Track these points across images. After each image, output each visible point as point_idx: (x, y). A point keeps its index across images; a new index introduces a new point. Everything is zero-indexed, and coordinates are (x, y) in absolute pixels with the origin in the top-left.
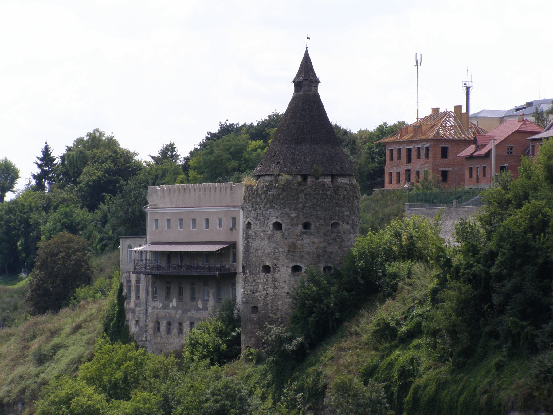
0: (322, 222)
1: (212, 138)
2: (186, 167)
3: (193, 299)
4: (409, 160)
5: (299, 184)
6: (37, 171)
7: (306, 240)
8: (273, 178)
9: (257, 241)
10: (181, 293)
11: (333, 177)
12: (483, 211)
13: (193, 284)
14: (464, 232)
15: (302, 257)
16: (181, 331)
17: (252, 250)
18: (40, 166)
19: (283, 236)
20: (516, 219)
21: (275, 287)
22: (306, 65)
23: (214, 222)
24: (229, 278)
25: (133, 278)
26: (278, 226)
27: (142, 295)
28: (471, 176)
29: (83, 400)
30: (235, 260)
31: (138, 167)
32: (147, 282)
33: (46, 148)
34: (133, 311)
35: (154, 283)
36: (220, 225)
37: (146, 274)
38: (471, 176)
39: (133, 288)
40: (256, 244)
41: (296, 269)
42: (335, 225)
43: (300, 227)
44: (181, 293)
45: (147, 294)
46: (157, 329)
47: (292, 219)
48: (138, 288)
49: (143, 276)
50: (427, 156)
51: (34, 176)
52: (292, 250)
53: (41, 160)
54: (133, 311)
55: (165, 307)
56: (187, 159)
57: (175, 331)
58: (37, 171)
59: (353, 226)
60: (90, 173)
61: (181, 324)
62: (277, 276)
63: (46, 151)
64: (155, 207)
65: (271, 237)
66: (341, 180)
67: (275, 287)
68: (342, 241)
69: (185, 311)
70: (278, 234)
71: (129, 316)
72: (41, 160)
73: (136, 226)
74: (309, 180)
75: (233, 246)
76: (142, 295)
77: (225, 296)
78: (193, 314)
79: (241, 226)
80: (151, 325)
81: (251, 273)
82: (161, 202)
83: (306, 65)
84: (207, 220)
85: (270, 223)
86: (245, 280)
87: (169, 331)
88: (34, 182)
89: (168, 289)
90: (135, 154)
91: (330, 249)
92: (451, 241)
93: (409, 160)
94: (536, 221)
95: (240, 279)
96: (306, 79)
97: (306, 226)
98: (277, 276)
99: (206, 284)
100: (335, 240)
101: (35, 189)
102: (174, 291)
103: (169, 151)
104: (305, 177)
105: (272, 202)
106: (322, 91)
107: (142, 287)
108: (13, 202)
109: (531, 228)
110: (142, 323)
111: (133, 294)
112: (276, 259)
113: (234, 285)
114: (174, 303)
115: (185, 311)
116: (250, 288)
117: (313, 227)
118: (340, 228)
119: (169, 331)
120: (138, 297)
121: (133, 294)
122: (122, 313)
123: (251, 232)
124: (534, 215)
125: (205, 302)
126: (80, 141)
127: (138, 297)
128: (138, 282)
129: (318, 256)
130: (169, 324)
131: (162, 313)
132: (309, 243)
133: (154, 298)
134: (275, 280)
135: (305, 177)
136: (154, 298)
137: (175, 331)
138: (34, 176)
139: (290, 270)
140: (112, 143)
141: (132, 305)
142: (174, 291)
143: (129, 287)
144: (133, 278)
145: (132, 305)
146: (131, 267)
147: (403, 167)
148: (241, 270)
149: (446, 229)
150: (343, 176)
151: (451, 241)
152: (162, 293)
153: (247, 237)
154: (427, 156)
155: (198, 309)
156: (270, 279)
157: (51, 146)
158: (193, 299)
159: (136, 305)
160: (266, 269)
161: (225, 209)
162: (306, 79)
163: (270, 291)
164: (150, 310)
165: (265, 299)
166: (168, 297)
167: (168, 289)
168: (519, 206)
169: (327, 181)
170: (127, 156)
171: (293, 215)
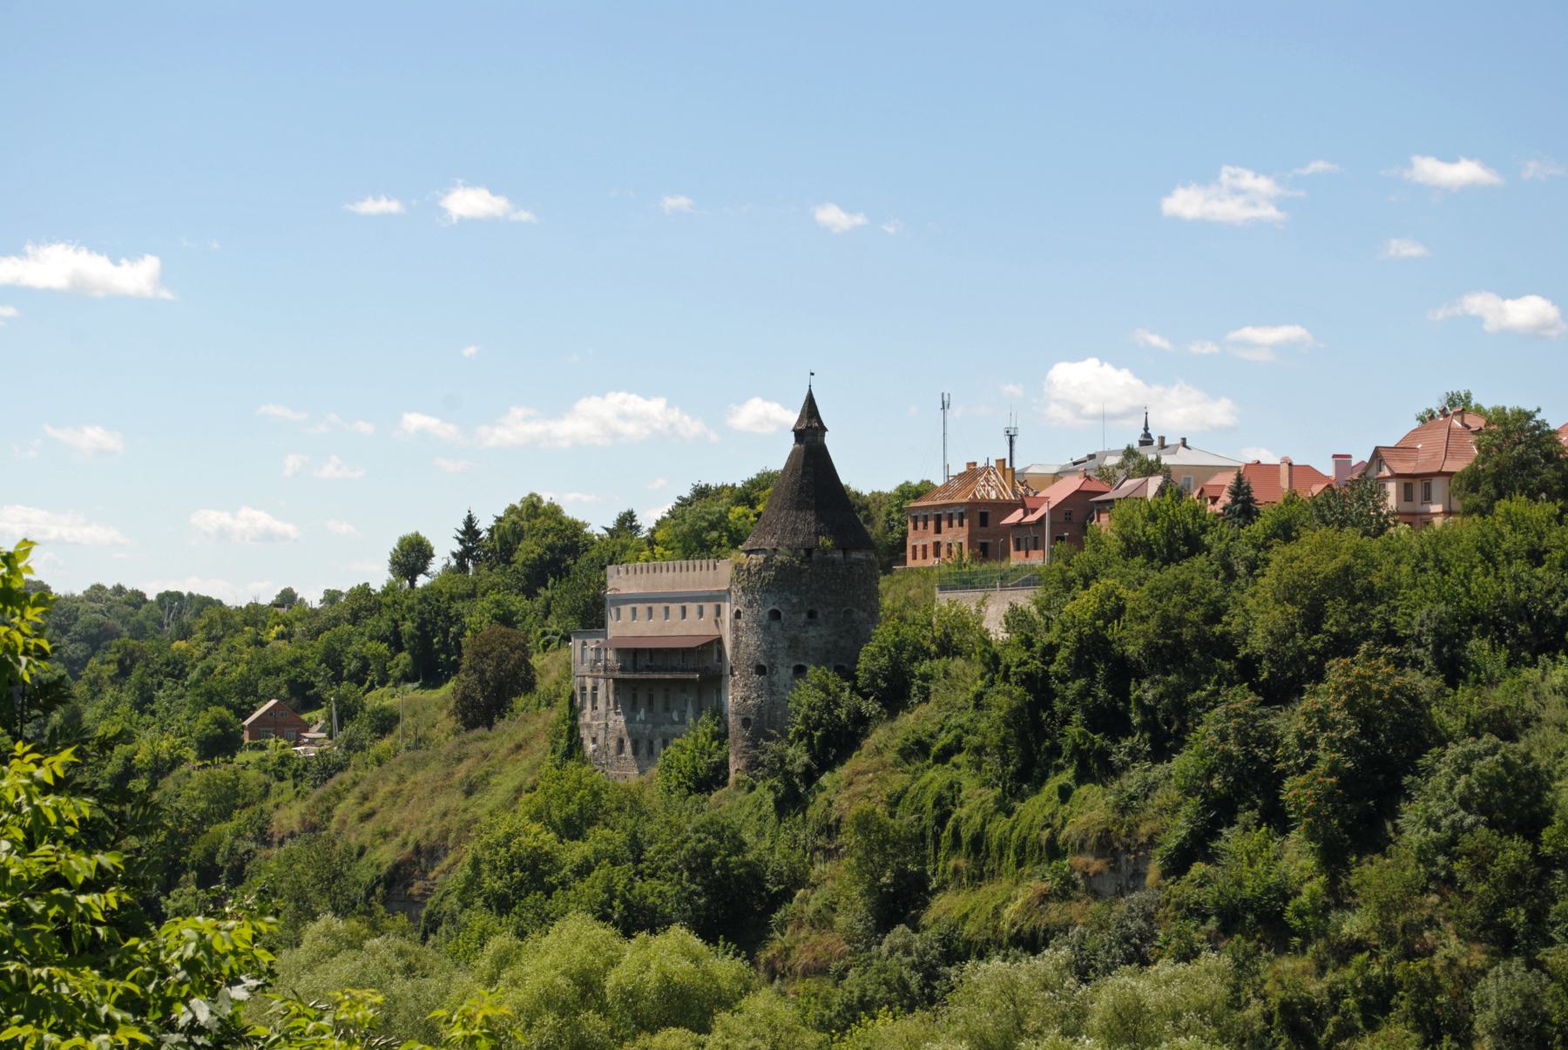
1: (684, 503)
2: (651, 542)
3: (667, 709)
7: (812, 632)
10: (651, 703)
12: (1039, 592)
15: (806, 654)
25: (589, 683)
29: (528, 841)
31: (590, 542)
39: (589, 697)
43: (804, 615)
44: (651, 703)
45: (608, 703)
46: (621, 748)
47: (794, 605)
48: (594, 696)
49: (601, 681)
52: (794, 644)
53: (463, 533)
54: (589, 726)
56: (653, 531)
58: (458, 548)
60: (528, 550)
61: (651, 743)
62: (775, 679)
66: (856, 555)
69: (656, 725)
71: (584, 733)
72: (463, 533)
76: (601, 706)
78: (667, 728)
80: (613, 744)
89: (635, 696)
92: (997, 631)
97: (812, 615)
98: (775, 679)
102: (642, 698)
103: (627, 522)
107: (601, 694)
110: (600, 741)
111: (589, 705)
113: (719, 691)
114: (642, 715)
115: (656, 725)
120: (594, 708)
121: (589, 705)
122: (573, 731)
125: (682, 713)
127: (594, 708)
128: (595, 688)
134: (772, 684)
139: (791, 671)
141: (587, 718)
142: (642, 698)
143: (583, 695)
150: (858, 549)
155: (673, 723)
157: (476, 515)
159: (593, 718)
167: (635, 696)
168: (1086, 587)
170: (577, 527)
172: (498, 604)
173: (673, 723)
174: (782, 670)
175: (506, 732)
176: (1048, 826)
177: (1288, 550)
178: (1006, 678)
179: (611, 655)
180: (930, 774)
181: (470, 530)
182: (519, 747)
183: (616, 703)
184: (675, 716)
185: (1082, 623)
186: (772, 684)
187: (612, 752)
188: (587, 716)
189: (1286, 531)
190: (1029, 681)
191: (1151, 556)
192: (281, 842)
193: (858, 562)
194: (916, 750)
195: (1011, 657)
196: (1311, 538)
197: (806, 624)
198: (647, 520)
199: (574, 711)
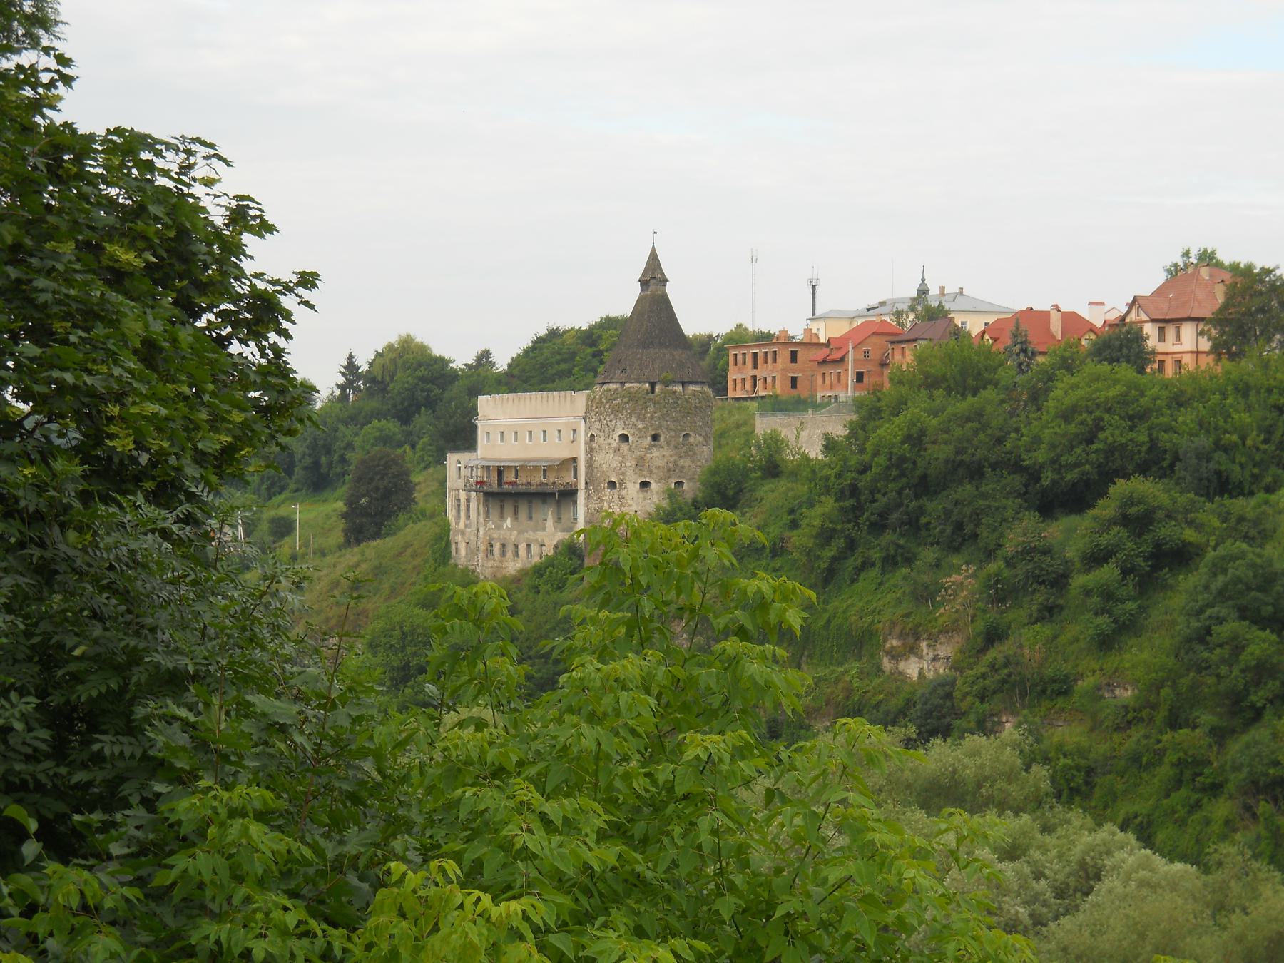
0: (673, 433)
7: (656, 453)
8: (618, 386)
9: (602, 455)
10: (516, 512)
11: (683, 383)
13: (530, 502)
14: (830, 445)
15: (651, 472)
16: (517, 554)
20: (890, 431)
21: (622, 505)
22: (653, 257)
23: (553, 434)
24: (568, 495)
25: (463, 496)
26: (624, 438)
30: (575, 477)
33: (351, 357)
34: (463, 533)
36: (560, 438)
39: (463, 507)
40: (599, 458)
41: (645, 485)
43: (649, 438)
44: (516, 512)
45: (479, 514)
47: (640, 430)
48: (468, 506)
49: (473, 494)
52: (640, 463)
54: (463, 533)
61: (516, 546)
62: (624, 492)
66: (691, 388)
68: (695, 454)
70: (625, 447)
73: (464, 437)
74: (658, 388)
76: (473, 514)
79: (582, 439)
80: (483, 547)
81: (595, 490)
82: (493, 412)
83: (653, 257)
84: (545, 432)
85: (616, 436)
86: (588, 497)
87: (503, 553)
91: (681, 462)
92: (815, 451)
94: (914, 431)
95: (581, 496)
96: (653, 277)
97: (655, 438)
98: (624, 492)
99: (544, 502)
102: (509, 509)
104: (653, 385)
105: (616, 411)
107: (473, 505)
109: (908, 438)
110: (472, 546)
112: (623, 474)
113: (575, 502)
114: (508, 523)
116: (593, 506)
117: (662, 439)
118: (691, 439)
119: (503, 553)
126: (390, 347)
128: (468, 500)
129: (669, 470)
130: (503, 545)
132: (660, 456)
135: (653, 385)
137: (510, 554)
140: (423, 349)
141: (462, 526)
142: (509, 509)
144: (463, 496)
145: (462, 526)
146: (461, 484)
148: (582, 485)
149: (807, 438)
150: (696, 383)
151: (815, 451)
152: (495, 513)
153: (590, 451)
156: (616, 497)
159: (466, 526)
160: (612, 485)
166: (502, 517)
169: (678, 388)
171: (641, 426)
172: (380, 430)
174: (630, 485)
177: (1069, 380)
181: (351, 366)
185: (893, 446)
191: (949, 390)
197: (651, 446)
198: (502, 362)
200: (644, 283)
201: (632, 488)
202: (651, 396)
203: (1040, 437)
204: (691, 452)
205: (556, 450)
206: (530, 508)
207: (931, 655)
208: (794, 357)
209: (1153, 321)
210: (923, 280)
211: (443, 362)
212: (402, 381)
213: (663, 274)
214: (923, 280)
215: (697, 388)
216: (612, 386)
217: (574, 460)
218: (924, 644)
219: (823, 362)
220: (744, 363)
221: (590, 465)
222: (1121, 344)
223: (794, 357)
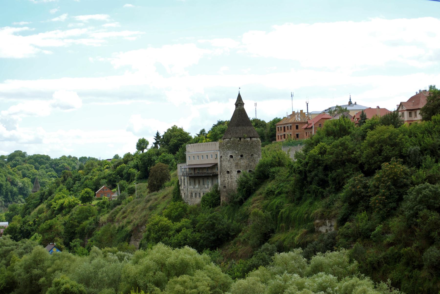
3: (204, 184)
4: (285, 131)
5: (238, 141)
6: (155, 141)
7: (242, 161)
8: (229, 139)
10: (199, 183)
11: (251, 138)
14: (297, 156)
16: (200, 196)
17: (223, 166)
18: (156, 140)
19: (233, 160)
20: (315, 151)
23: (210, 156)
24: (215, 176)
26: (231, 157)
27: (186, 184)
28: (307, 135)
30: (217, 170)
32: (187, 179)
34: (183, 190)
35: (190, 179)
37: (187, 176)
38: (307, 135)
39: (183, 182)
40: (224, 163)
41: (239, 172)
42: (252, 155)
43: (240, 157)
44: (199, 183)
47: (236, 154)
48: (184, 181)
49: (186, 177)
50: (291, 129)
51: (154, 143)
52: (237, 165)
54: (183, 190)
55: (194, 188)
57: (198, 196)
59: (259, 155)
61: (200, 194)
62: (232, 175)
63: (158, 134)
64: (189, 152)
65: (229, 161)
66: (253, 139)
67: (232, 179)
70: (232, 159)
71: (182, 192)
73: (184, 160)
74: (242, 139)
75: (217, 164)
76: (186, 184)
77: (215, 183)
78: (204, 190)
79: (219, 157)
80: (189, 195)
81: (223, 174)
85: (229, 156)
86: (221, 177)
87: (196, 197)
88: (154, 146)
89: (195, 181)
90: (189, 133)
91: (250, 164)
93: (285, 131)
95: (219, 176)
96: (239, 103)
97: (242, 156)
98: (232, 175)
99: (208, 179)
100: (252, 161)
101: (154, 148)
102: (197, 182)
105: (229, 148)
106: (246, 107)
108: (146, 153)
109: (320, 153)
110: (186, 194)
111: (183, 184)
112: (231, 168)
113: (217, 178)
114: (197, 186)
116: (222, 179)
118: (254, 156)
119: (196, 197)
121: (183, 184)
122: (179, 191)
123: (222, 159)
124: (321, 148)
128: (184, 179)
129: (247, 167)
130: (196, 194)
131: (193, 190)
132: (243, 162)
133: (190, 185)
134: (231, 176)
135: (240, 139)
136: (190, 185)
137: (198, 196)
138: (154, 143)
141: (183, 188)
142: (197, 182)
143: (181, 181)
144: (183, 178)
145: (183, 188)
146: (181, 174)
147: (283, 133)
148: (219, 173)
150: (254, 137)
152: (193, 183)
153: (221, 161)
154: (291, 129)
155: (206, 188)
158: (204, 184)
159: (184, 188)
160: (228, 172)
161: (213, 151)
162: (239, 103)
163: (230, 180)
164: (189, 189)
165: (228, 183)
166: (195, 184)
167: (195, 181)
168: (316, 145)
169: (249, 139)
171: (237, 152)
173: (206, 188)
174: (234, 172)
175: (161, 193)
176: (306, 213)
177: (372, 132)
178: (294, 172)
179: (187, 170)
180: (275, 200)
182: (165, 196)
183: (190, 183)
184: (206, 186)
186: (231, 176)
187: (189, 197)
188: (182, 188)
189: (372, 128)
190: (300, 172)
191: (335, 136)
192: (102, 225)
193: (254, 141)
194: (270, 193)
195: (295, 165)
196: (380, 128)
199: (179, 186)
200: (237, 105)
201: (235, 173)
202: (239, 142)
203: (362, 151)
204: (253, 160)
205: (211, 161)
206: (203, 181)
207: (330, 225)
208: (297, 127)
209: (407, 110)
210: (350, 100)
211: (186, 134)
212: (174, 141)
213: (242, 102)
214: (350, 100)
215: (255, 139)
216: (227, 140)
217: (217, 164)
218: (327, 221)
219: (306, 129)
220: (281, 130)
221: (221, 166)
222: (391, 119)
223: (297, 127)
